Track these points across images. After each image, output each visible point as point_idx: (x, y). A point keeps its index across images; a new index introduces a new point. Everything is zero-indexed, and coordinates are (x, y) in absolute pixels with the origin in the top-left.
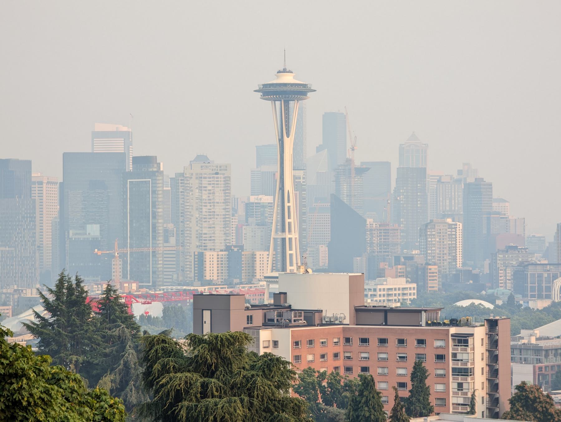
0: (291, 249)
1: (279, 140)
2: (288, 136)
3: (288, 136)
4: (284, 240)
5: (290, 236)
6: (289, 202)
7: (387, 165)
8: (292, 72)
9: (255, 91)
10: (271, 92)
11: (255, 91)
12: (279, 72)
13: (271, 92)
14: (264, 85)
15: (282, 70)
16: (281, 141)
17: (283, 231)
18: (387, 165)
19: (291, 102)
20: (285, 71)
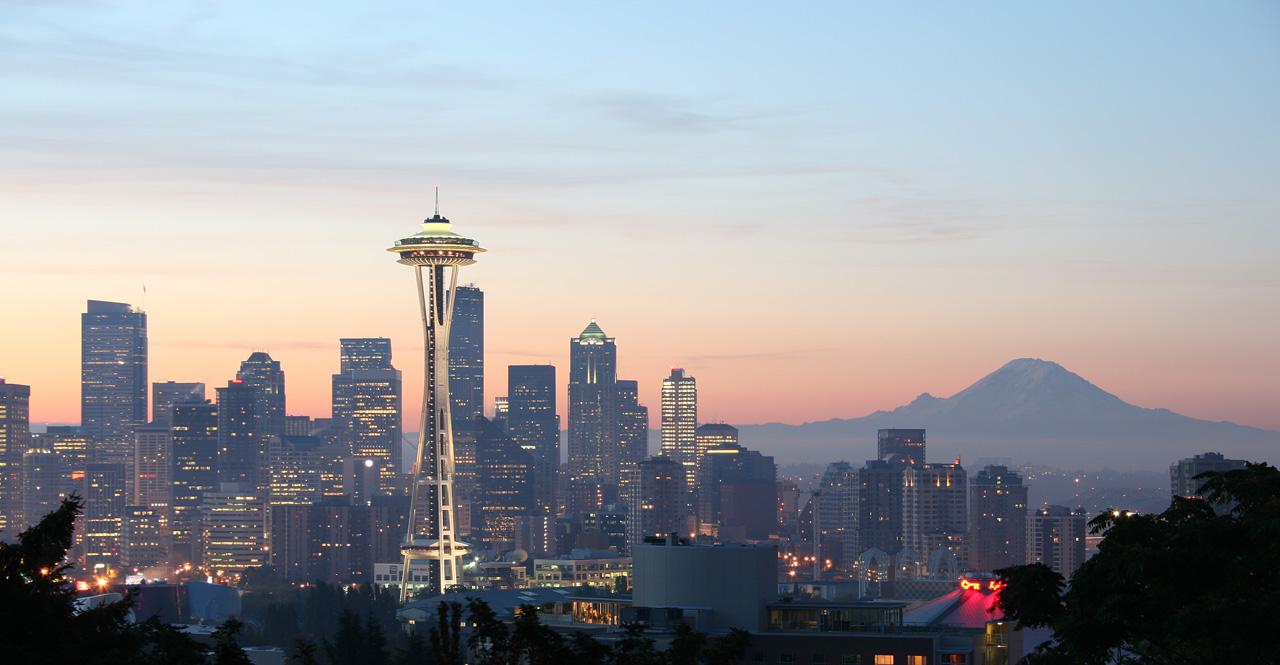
0: (445, 503)
1: (428, 328)
2: (441, 323)
3: (441, 323)
4: (435, 487)
5: (443, 483)
6: (442, 427)
7: (549, 371)
8: (447, 221)
9: (388, 250)
10: (410, 252)
11: (388, 250)
12: (428, 221)
13: (410, 252)
14: (404, 242)
15: (432, 217)
16: (431, 328)
17: (435, 476)
18: (549, 371)
19: (447, 272)
20: (437, 219)
